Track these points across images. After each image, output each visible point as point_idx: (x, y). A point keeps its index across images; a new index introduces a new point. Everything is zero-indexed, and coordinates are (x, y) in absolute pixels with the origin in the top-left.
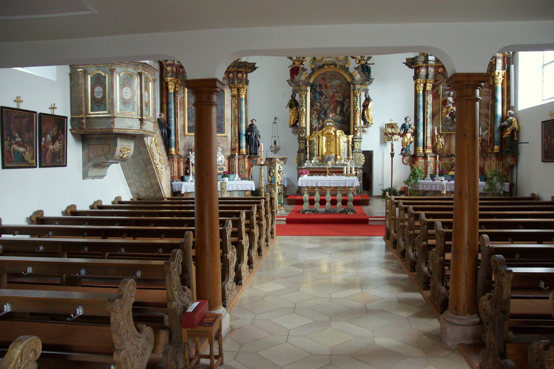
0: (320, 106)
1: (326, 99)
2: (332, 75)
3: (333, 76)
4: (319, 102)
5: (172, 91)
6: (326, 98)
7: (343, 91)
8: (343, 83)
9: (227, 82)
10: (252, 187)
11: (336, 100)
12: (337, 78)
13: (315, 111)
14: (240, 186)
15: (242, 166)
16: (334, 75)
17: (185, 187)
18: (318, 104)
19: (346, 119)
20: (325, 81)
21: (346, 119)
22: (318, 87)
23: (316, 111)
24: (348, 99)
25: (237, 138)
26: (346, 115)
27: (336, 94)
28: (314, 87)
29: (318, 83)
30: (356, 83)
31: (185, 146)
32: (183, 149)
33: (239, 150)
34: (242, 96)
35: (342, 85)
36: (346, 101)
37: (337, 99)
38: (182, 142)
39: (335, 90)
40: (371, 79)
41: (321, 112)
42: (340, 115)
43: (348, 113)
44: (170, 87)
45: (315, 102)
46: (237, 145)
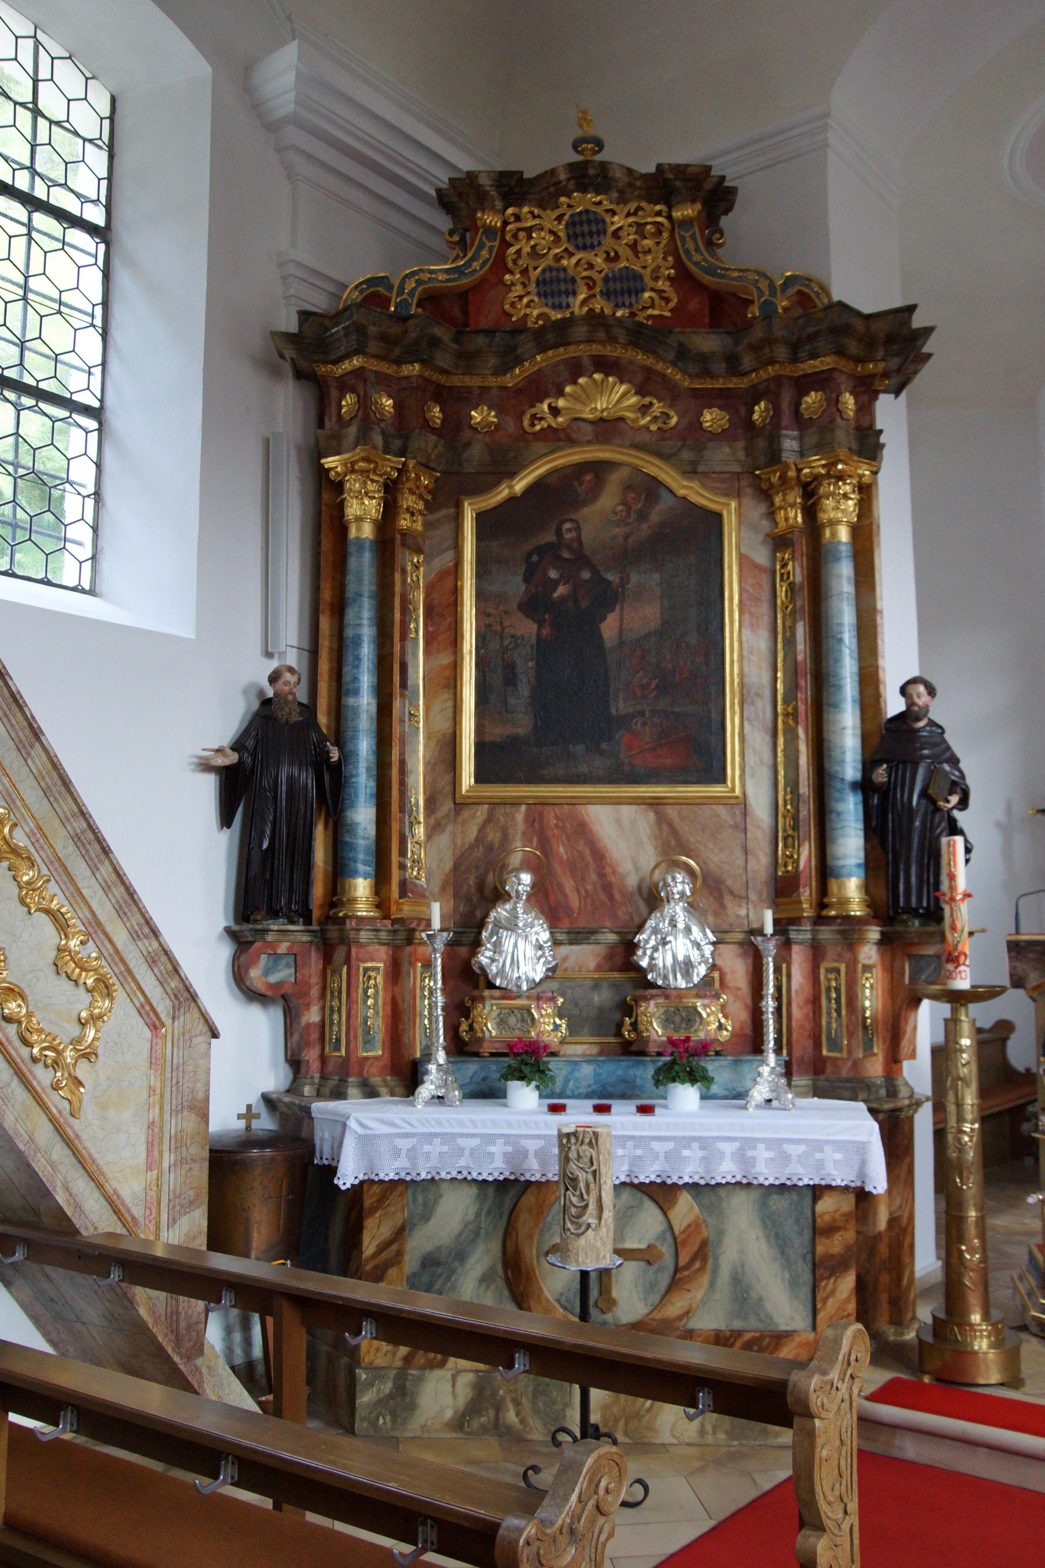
5: (367, 531)
9: (741, 455)
10: (863, 1163)
14: (762, 1154)
15: (838, 1000)
17: (366, 1142)
25: (807, 810)
31: (456, 866)
32: (443, 889)
33: (823, 889)
34: (834, 534)
38: (443, 840)
44: (353, 509)
46: (806, 854)
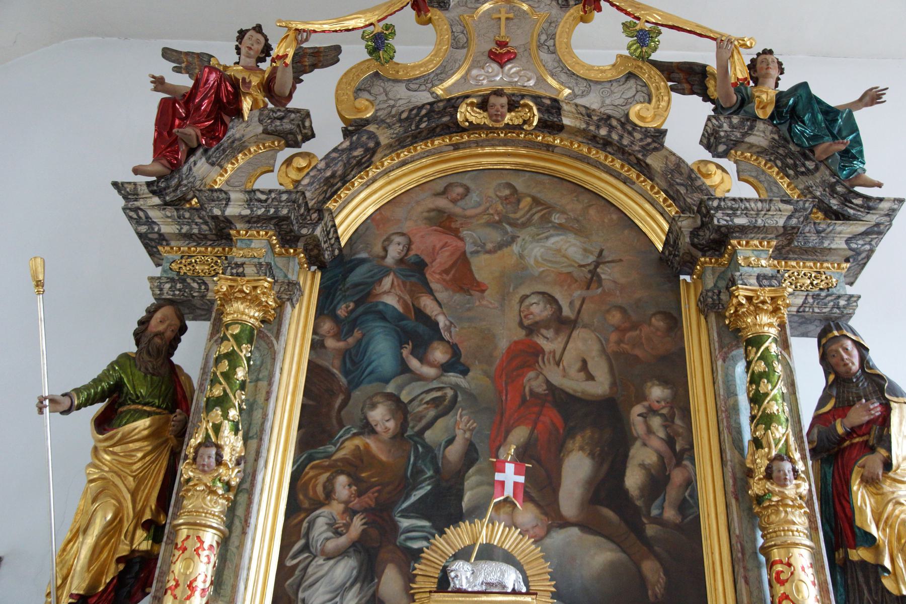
0: (399, 436)
1: (453, 378)
2: (515, 196)
3: (526, 202)
4: (394, 399)
6: (455, 364)
7: (616, 318)
8: (608, 256)
11: (548, 382)
12: (556, 218)
13: (342, 480)
16: (536, 201)
18: (379, 415)
19: (651, 569)
20: (456, 233)
21: (651, 569)
22: (387, 282)
23: (355, 480)
24: (664, 382)
26: (651, 530)
27: (548, 343)
28: (357, 276)
29: (394, 252)
30: (740, 221)
35: (605, 273)
36: (641, 397)
37: (556, 379)
39: (539, 310)
40: (869, 204)
41: (407, 485)
42: (587, 526)
43: (670, 514)
45: (357, 394)
